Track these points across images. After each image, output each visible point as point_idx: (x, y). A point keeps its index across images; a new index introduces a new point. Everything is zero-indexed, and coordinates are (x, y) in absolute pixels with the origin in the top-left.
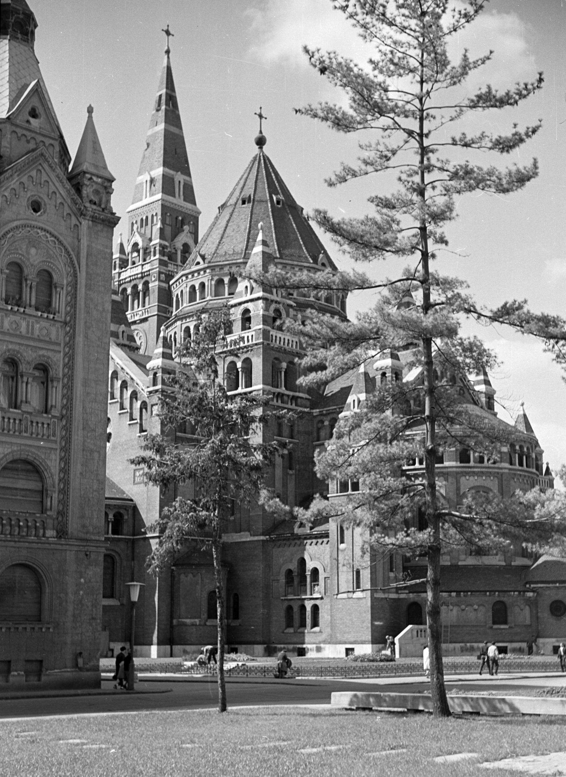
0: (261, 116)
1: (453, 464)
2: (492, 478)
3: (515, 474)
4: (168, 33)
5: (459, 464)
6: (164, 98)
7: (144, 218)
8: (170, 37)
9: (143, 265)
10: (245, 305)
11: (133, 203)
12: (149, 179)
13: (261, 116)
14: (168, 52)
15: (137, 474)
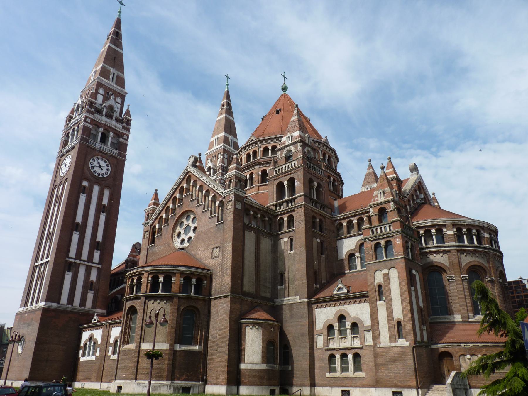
0: (284, 77)
1: (454, 244)
2: (482, 256)
3: (496, 255)
4: (228, 77)
5: (457, 244)
6: (225, 104)
7: (214, 156)
8: (229, 79)
9: (212, 177)
10: (288, 148)
11: (208, 150)
12: (217, 138)
13: (284, 77)
14: (228, 85)
15: (215, 251)
